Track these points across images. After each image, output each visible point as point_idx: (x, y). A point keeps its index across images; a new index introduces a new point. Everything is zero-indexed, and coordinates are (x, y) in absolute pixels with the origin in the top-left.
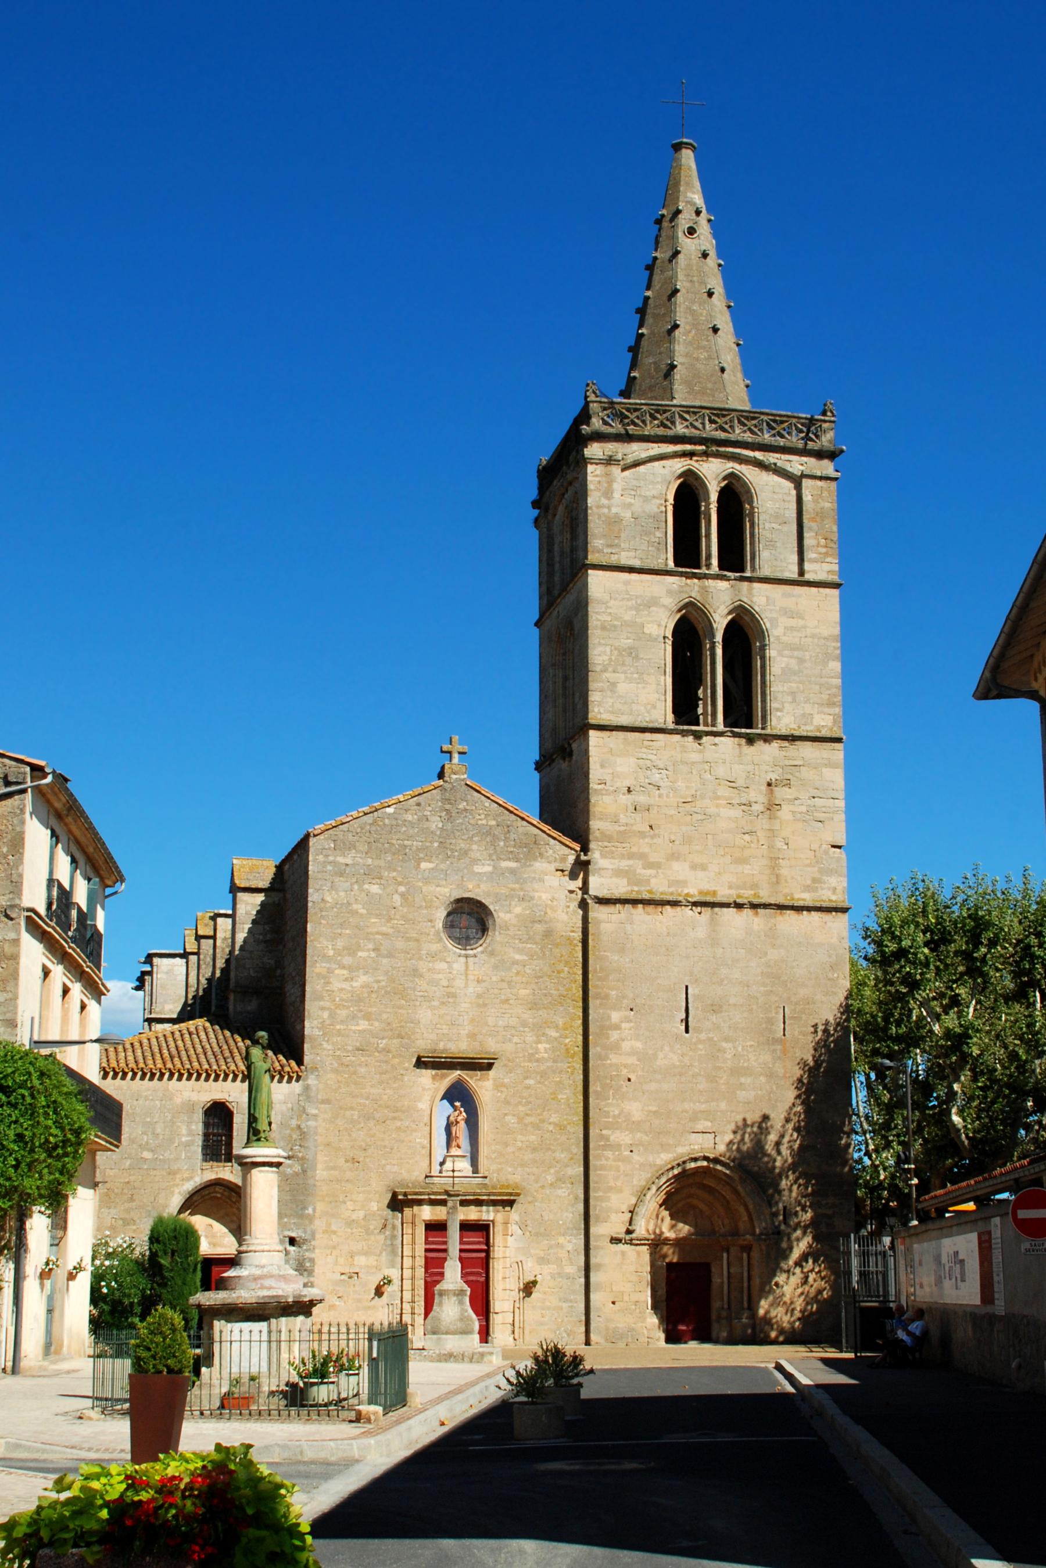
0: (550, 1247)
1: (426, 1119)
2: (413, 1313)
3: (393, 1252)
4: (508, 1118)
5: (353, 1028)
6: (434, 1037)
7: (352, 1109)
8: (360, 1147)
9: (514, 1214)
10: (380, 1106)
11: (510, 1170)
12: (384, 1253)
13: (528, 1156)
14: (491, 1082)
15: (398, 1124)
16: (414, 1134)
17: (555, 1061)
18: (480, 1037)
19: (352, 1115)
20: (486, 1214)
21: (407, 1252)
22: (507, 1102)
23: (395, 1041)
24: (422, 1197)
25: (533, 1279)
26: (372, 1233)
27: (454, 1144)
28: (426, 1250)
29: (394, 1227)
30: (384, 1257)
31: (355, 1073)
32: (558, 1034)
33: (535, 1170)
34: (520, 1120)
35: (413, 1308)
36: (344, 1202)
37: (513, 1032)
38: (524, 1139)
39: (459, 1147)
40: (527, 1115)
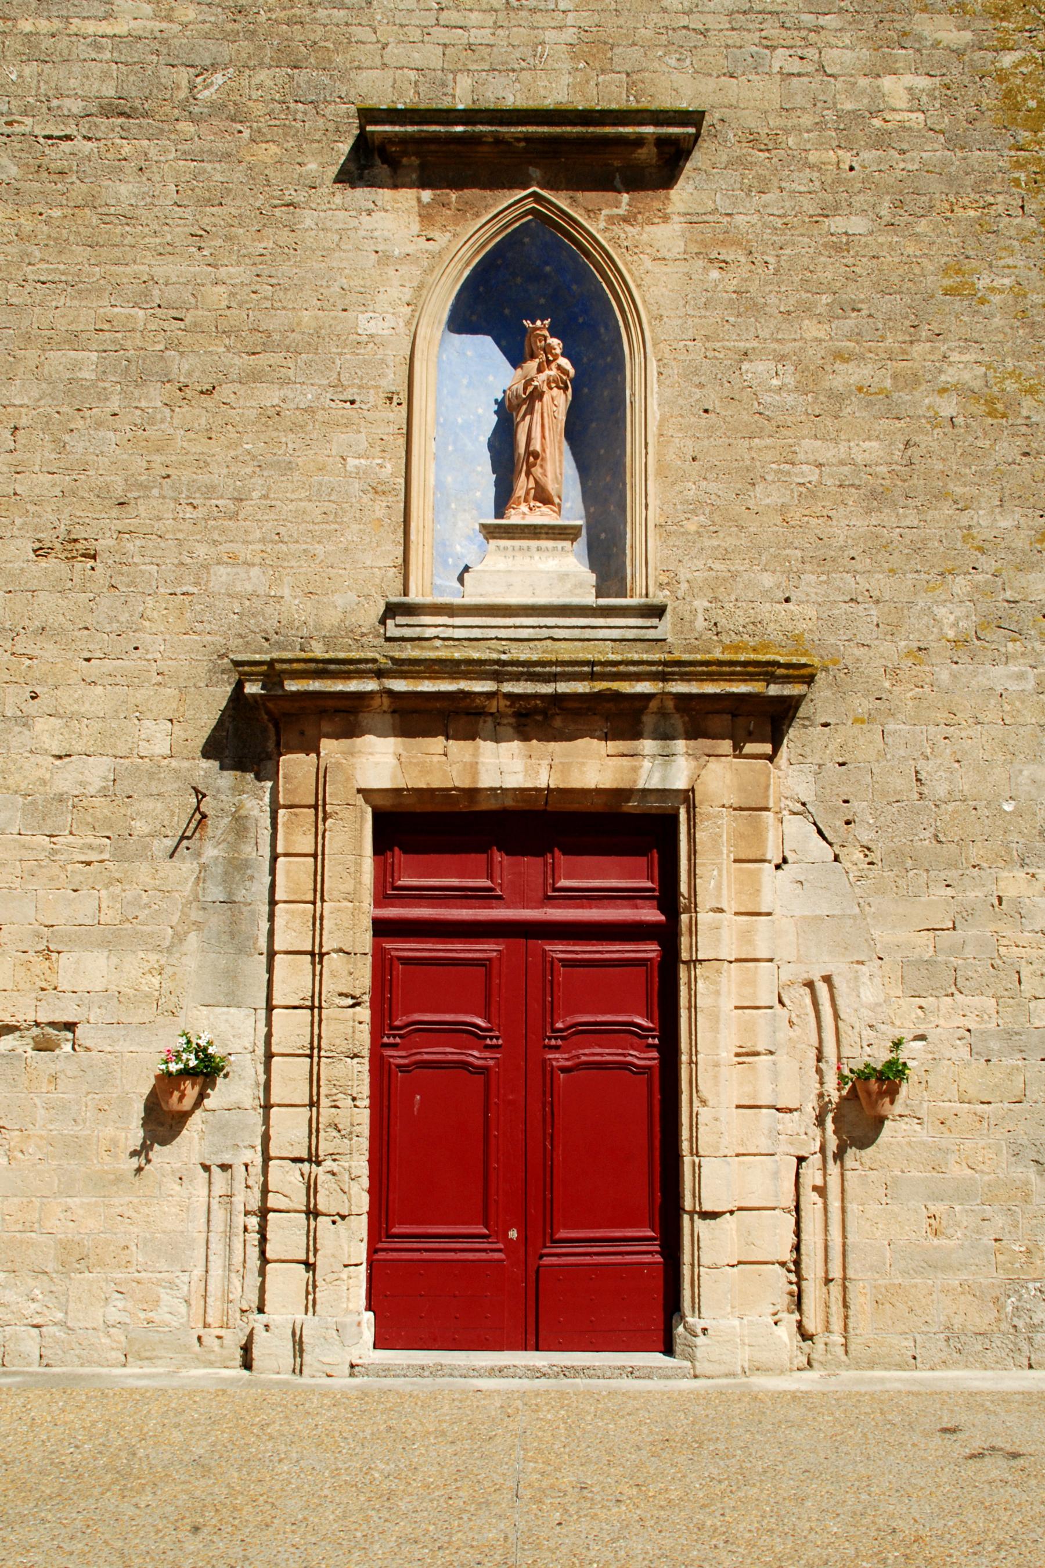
0: (964, 916)
1: (393, 379)
2: (312, 1213)
3: (234, 935)
4: (758, 369)
5: (91, 27)
6: (430, 56)
7: (74, 339)
8: (102, 493)
9: (792, 773)
10: (196, 328)
11: (767, 580)
12: (193, 939)
13: (849, 524)
14: (676, 226)
15: (271, 396)
16: (340, 438)
17: (955, 142)
18: (627, 57)
19: (76, 365)
20: (659, 766)
21: (291, 932)
22: (746, 305)
23: (263, 76)
24: (353, 686)
25: (880, 1057)
26: (144, 853)
27: (522, 485)
28: (382, 928)
29: (240, 825)
30: (193, 958)
31: (91, 203)
32: (968, 36)
33: (879, 582)
34: (810, 378)
35: (311, 1188)
36: (25, 721)
37: (772, 30)
38: (828, 453)
39: (543, 497)
40: (840, 356)
